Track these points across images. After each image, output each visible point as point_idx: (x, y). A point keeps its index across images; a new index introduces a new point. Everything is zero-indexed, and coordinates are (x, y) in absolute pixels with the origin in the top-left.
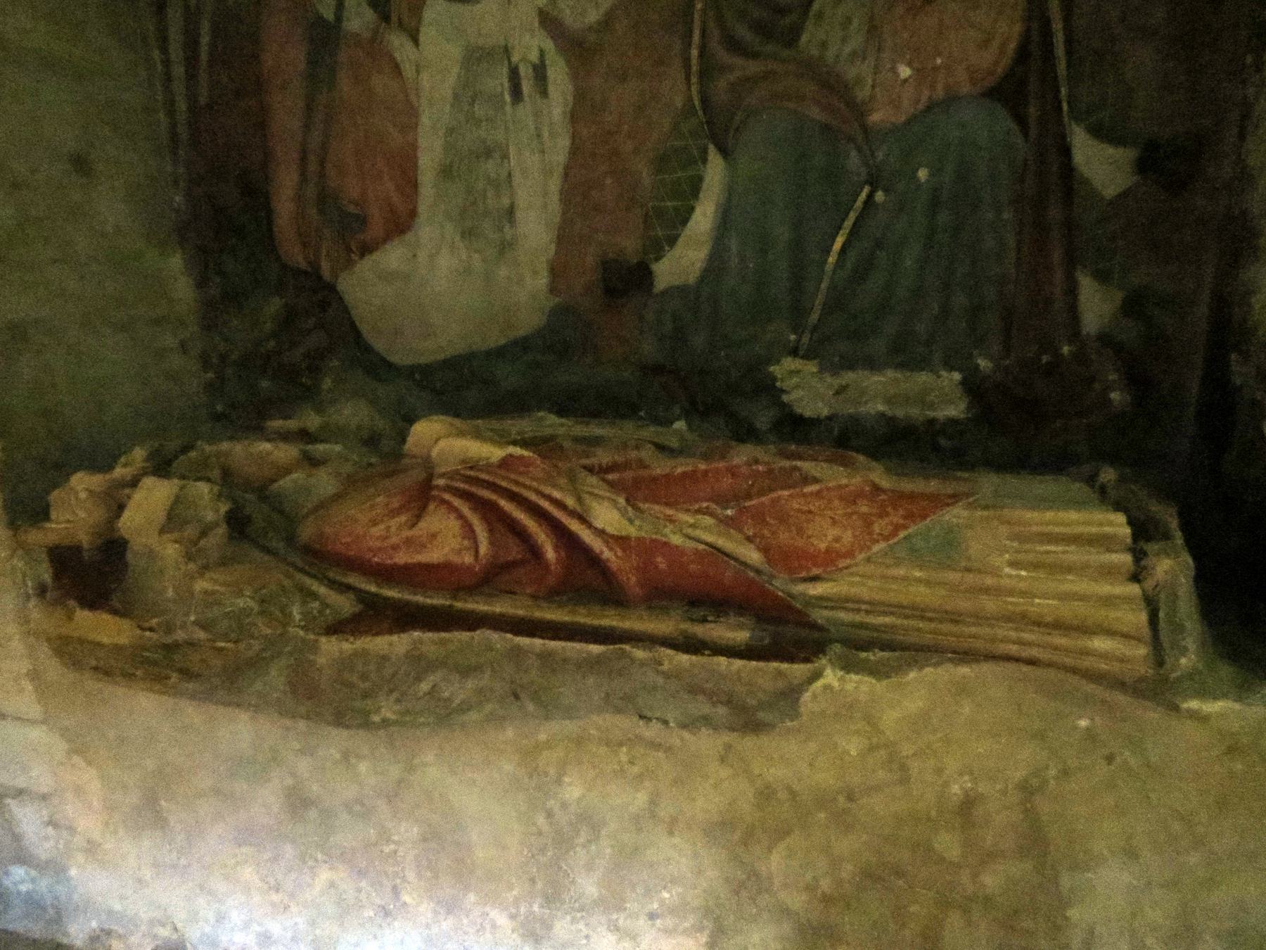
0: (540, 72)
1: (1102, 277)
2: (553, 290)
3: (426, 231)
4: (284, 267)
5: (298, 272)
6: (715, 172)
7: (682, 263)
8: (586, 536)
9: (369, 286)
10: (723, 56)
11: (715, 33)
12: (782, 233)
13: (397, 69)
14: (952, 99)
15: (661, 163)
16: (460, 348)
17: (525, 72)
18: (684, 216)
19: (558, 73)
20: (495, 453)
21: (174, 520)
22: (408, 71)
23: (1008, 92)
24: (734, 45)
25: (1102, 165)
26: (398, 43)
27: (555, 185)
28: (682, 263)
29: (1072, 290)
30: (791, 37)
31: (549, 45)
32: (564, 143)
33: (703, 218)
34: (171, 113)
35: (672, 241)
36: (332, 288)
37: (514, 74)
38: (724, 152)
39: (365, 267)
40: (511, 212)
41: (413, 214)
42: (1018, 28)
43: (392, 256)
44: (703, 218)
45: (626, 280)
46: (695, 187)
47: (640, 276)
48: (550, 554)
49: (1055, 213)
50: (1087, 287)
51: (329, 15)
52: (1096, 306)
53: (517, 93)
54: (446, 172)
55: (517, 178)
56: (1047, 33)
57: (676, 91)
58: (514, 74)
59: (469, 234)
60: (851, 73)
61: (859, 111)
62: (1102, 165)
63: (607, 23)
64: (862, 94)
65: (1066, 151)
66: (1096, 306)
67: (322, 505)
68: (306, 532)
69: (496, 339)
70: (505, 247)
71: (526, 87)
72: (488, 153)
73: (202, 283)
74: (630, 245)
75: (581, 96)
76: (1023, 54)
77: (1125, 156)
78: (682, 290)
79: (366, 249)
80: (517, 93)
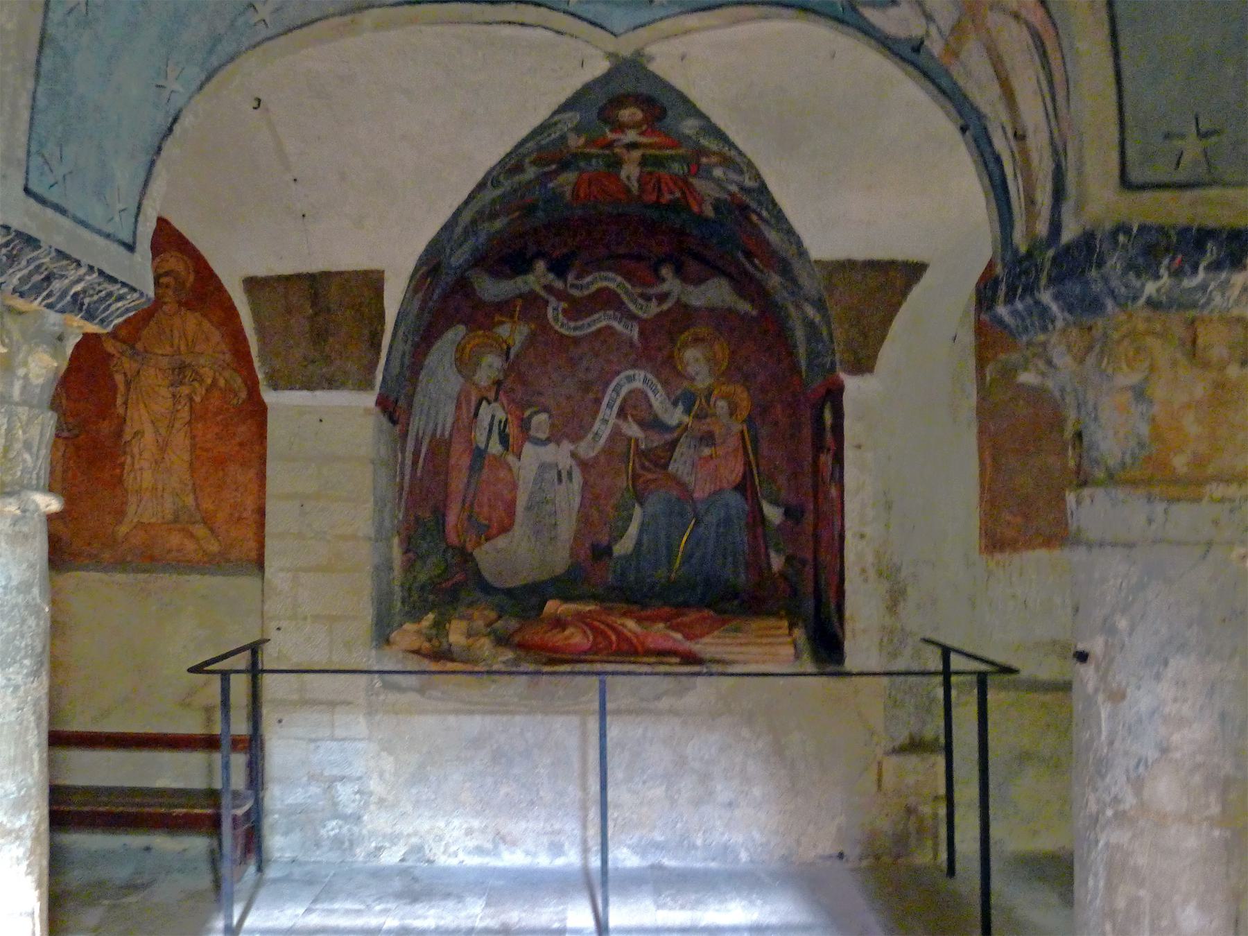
0: (570, 474)
1: (778, 551)
2: (571, 556)
3: (517, 530)
5: (454, 548)
6: (637, 511)
7: (623, 547)
8: (625, 631)
9: (487, 556)
10: (641, 472)
11: (637, 466)
12: (662, 535)
13: (510, 469)
14: (721, 490)
16: (530, 579)
17: (564, 474)
20: (588, 608)
22: (515, 470)
26: (511, 458)
27: (574, 516)
28: (623, 547)
29: (768, 556)
30: (665, 466)
31: (574, 463)
32: (578, 499)
33: (633, 529)
34: (402, 479)
36: (471, 554)
37: (559, 474)
38: (641, 504)
39: (487, 546)
41: (512, 524)
42: (742, 469)
43: (501, 542)
44: (633, 529)
45: (601, 553)
46: (630, 518)
47: (608, 551)
48: (614, 638)
49: (759, 530)
50: (773, 554)
51: (482, 446)
52: (777, 562)
53: (560, 480)
54: (529, 508)
56: (751, 471)
57: (623, 482)
58: (559, 474)
59: (537, 533)
60: (686, 479)
62: (773, 514)
63: (597, 457)
64: (691, 487)
65: (761, 510)
66: (777, 562)
67: (516, 632)
68: (517, 639)
69: (545, 577)
70: (553, 539)
72: (547, 502)
73: (406, 552)
74: (604, 539)
75: (585, 483)
76: (744, 477)
77: (782, 510)
79: (487, 540)
80: (560, 480)
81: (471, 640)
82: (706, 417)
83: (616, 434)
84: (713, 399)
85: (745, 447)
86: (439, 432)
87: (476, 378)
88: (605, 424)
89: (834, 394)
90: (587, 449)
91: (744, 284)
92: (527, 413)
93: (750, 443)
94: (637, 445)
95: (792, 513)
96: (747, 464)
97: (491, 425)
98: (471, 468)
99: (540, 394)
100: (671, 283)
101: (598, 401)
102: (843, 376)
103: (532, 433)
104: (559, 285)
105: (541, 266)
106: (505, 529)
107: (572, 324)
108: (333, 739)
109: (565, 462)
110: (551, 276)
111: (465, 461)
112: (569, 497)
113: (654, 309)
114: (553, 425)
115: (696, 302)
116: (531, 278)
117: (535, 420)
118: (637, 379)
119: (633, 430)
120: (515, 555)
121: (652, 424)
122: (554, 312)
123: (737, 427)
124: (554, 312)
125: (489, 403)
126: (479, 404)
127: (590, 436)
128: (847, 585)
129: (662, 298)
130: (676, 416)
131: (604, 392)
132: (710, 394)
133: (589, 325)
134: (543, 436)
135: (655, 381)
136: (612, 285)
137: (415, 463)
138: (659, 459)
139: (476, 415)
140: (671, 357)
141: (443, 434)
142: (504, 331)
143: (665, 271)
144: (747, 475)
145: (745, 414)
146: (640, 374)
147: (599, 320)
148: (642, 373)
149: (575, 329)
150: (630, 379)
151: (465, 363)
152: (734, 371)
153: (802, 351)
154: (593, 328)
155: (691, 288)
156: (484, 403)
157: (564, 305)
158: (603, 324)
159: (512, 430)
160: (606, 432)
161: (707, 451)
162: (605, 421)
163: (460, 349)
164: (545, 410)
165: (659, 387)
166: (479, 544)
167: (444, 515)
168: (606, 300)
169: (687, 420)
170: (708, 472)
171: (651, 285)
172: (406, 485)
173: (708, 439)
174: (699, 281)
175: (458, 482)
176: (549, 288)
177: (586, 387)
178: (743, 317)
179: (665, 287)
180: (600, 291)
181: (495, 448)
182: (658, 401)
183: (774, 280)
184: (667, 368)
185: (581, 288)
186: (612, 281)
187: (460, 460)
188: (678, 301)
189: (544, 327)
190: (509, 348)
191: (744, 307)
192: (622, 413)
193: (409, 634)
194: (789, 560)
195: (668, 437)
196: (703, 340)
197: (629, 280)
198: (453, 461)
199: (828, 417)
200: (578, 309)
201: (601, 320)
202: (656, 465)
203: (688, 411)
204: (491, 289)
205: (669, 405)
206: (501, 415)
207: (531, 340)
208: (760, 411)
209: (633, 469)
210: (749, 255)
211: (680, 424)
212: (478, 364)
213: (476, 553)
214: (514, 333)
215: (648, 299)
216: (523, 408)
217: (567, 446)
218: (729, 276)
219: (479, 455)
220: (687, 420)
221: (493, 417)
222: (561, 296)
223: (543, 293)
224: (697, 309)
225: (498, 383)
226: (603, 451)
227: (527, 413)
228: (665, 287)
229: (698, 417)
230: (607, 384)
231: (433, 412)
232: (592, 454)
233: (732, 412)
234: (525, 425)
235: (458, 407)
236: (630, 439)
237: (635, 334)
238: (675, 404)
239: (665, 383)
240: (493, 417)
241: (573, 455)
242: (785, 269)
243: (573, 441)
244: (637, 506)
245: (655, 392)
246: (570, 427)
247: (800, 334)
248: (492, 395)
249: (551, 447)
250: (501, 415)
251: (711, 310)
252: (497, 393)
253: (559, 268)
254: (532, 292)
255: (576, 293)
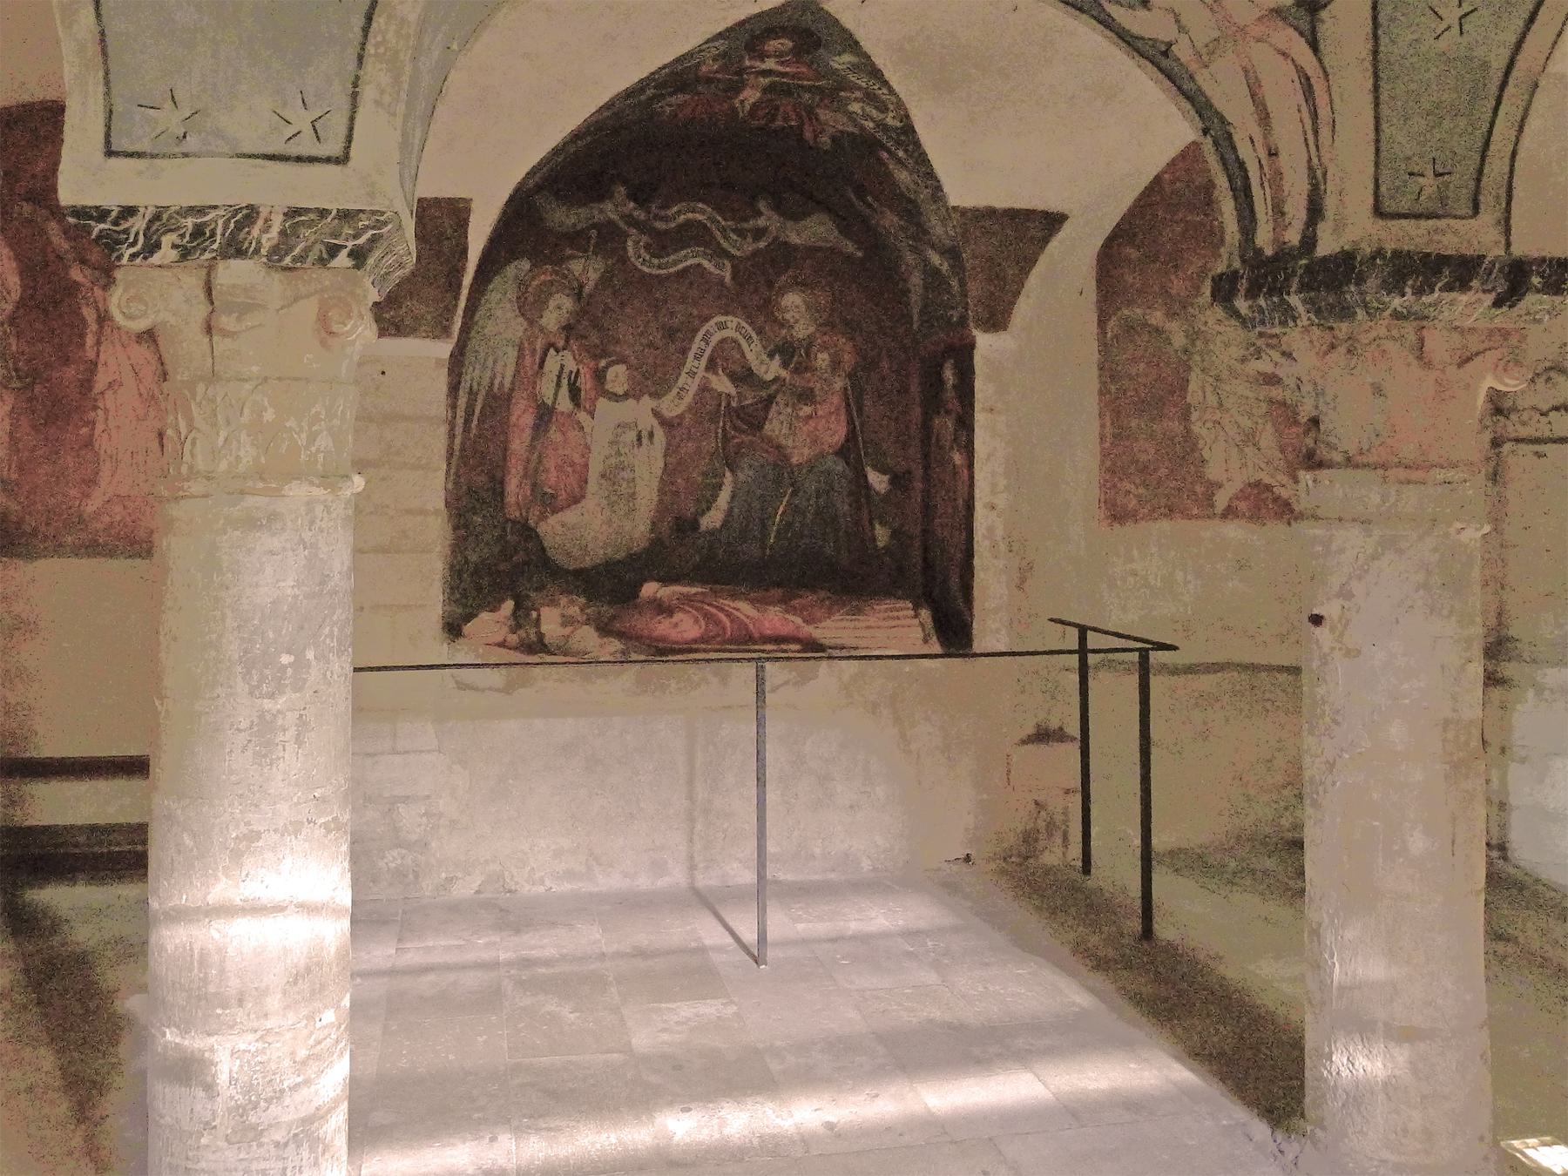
0: (651, 435)
2: (652, 531)
4: (508, 520)
5: (514, 522)
9: (555, 530)
14: (822, 455)
15: (705, 474)
17: (645, 434)
18: (715, 497)
19: (660, 434)
21: (567, 621)
23: (842, 452)
24: (735, 428)
25: (878, 481)
28: (712, 519)
30: (760, 427)
31: (655, 422)
33: (724, 497)
35: (709, 509)
38: (732, 471)
39: (553, 520)
40: (633, 496)
43: (570, 516)
45: (686, 526)
47: (695, 525)
50: (877, 526)
51: (549, 402)
52: (882, 535)
55: (638, 481)
59: (611, 505)
61: (787, 458)
62: (878, 481)
63: (681, 417)
66: (882, 535)
69: (621, 555)
71: (645, 441)
74: (691, 509)
75: (669, 444)
77: (886, 478)
78: (711, 533)
79: (554, 512)
81: (569, 630)
82: (806, 369)
83: (704, 388)
84: (815, 349)
85: (848, 405)
86: (497, 382)
87: (543, 321)
88: (693, 377)
89: (963, 354)
90: (672, 406)
91: (848, 221)
92: (603, 363)
93: (853, 402)
94: (729, 404)
95: (899, 480)
96: (850, 422)
97: (559, 377)
98: (536, 428)
99: (618, 342)
100: (768, 219)
101: (684, 351)
102: (975, 332)
103: (608, 387)
104: (640, 215)
105: (621, 191)
106: (576, 500)
107: (656, 261)
108: (394, 752)
109: (648, 422)
110: (632, 205)
111: (528, 420)
112: (648, 468)
113: (749, 247)
114: (631, 378)
115: (794, 239)
116: (608, 206)
117: (610, 374)
118: (728, 327)
119: (722, 384)
120: (588, 529)
121: (744, 377)
122: (634, 248)
123: (839, 384)
124: (634, 248)
125: (557, 351)
126: (545, 354)
127: (675, 391)
128: (976, 561)
129: (759, 233)
130: (771, 369)
131: (691, 340)
132: (810, 345)
133: (675, 263)
134: (621, 392)
135: (749, 329)
136: (700, 217)
137: (467, 421)
138: (753, 419)
139: (541, 366)
140: (768, 301)
141: (501, 384)
142: (576, 266)
143: (762, 206)
144: (851, 436)
145: (847, 367)
146: (732, 321)
147: (686, 258)
148: (736, 320)
149: (659, 267)
150: (722, 326)
151: (529, 306)
152: (834, 321)
153: (915, 299)
154: (680, 266)
155: (790, 224)
156: (552, 351)
157: (645, 239)
158: (690, 262)
159: (586, 383)
160: (693, 388)
161: (807, 410)
162: (692, 374)
163: (522, 284)
164: (622, 360)
165: (754, 335)
166: (542, 517)
167: (502, 482)
168: (692, 235)
169: (784, 373)
170: (809, 433)
171: (746, 220)
172: (457, 447)
173: (806, 396)
174: (796, 217)
175: (519, 444)
176: (630, 220)
177: (670, 333)
178: (849, 258)
179: (761, 222)
180: (689, 224)
181: (564, 404)
182: (754, 353)
183: (889, 220)
184: (764, 314)
185: (665, 219)
186: (701, 213)
187: (522, 417)
188: (776, 238)
189: (624, 260)
190: (581, 287)
191: (849, 247)
192: (711, 366)
193: (491, 624)
194: (895, 534)
195: (764, 394)
196: (804, 284)
197: (719, 210)
198: (513, 419)
199: (949, 374)
200: (663, 244)
201: (689, 258)
202: (751, 425)
203: (785, 365)
204: (563, 217)
205: (765, 357)
206: (571, 365)
207: (605, 280)
208: (867, 364)
209: (724, 430)
210: (860, 191)
211: (776, 379)
212: (546, 302)
213: (542, 529)
214: (587, 269)
215: (741, 233)
216: (596, 357)
217: (647, 402)
218: (829, 210)
219: (545, 414)
220: (784, 373)
221: (562, 366)
222: (642, 227)
223: (622, 224)
224: (796, 248)
225: (568, 329)
226: (690, 409)
227: (603, 363)
228: (761, 222)
229: (797, 371)
230: (696, 331)
231: (490, 363)
232: (679, 411)
233: (836, 364)
234: (599, 376)
235: (520, 357)
236: (720, 395)
237: (728, 276)
238: (771, 356)
239: (760, 332)
240: (562, 366)
241: (656, 413)
242: (910, 210)
243: (656, 395)
244: (728, 474)
245: (749, 339)
246: (651, 382)
247: (916, 280)
248: (561, 343)
249: (631, 402)
250: (571, 365)
251: (812, 250)
252: (567, 341)
253: (640, 195)
254: (610, 222)
255: (660, 225)
